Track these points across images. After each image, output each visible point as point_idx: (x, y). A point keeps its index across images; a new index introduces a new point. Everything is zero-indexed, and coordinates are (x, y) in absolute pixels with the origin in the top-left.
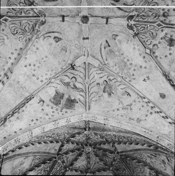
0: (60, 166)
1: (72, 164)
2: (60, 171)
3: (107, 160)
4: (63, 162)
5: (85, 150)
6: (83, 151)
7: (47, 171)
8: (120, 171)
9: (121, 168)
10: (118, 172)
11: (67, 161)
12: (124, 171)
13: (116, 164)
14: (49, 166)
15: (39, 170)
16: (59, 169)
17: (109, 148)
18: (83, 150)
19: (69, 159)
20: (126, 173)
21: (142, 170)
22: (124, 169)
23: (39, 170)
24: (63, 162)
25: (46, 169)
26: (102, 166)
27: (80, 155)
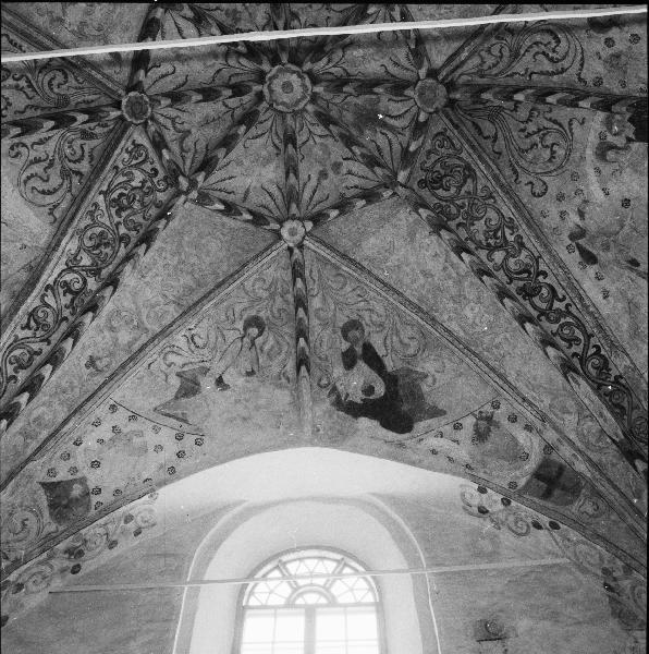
0: (147, 167)
1: (207, 165)
2: (147, 194)
3: (381, 141)
4: (159, 144)
5: (271, 91)
6: (260, 97)
7: (78, 173)
8: (448, 190)
9: (451, 170)
10: (440, 192)
11: (182, 150)
12: (469, 180)
13: (429, 152)
14: (86, 148)
15: (37, 161)
16: (144, 182)
17: (391, 68)
18: (257, 88)
19: (189, 142)
20: (480, 187)
21: (561, 152)
22: (468, 167)
23: (37, 161)
24: (159, 144)
25: (72, 165)
26: (356, 181)
27: (249, 118)
